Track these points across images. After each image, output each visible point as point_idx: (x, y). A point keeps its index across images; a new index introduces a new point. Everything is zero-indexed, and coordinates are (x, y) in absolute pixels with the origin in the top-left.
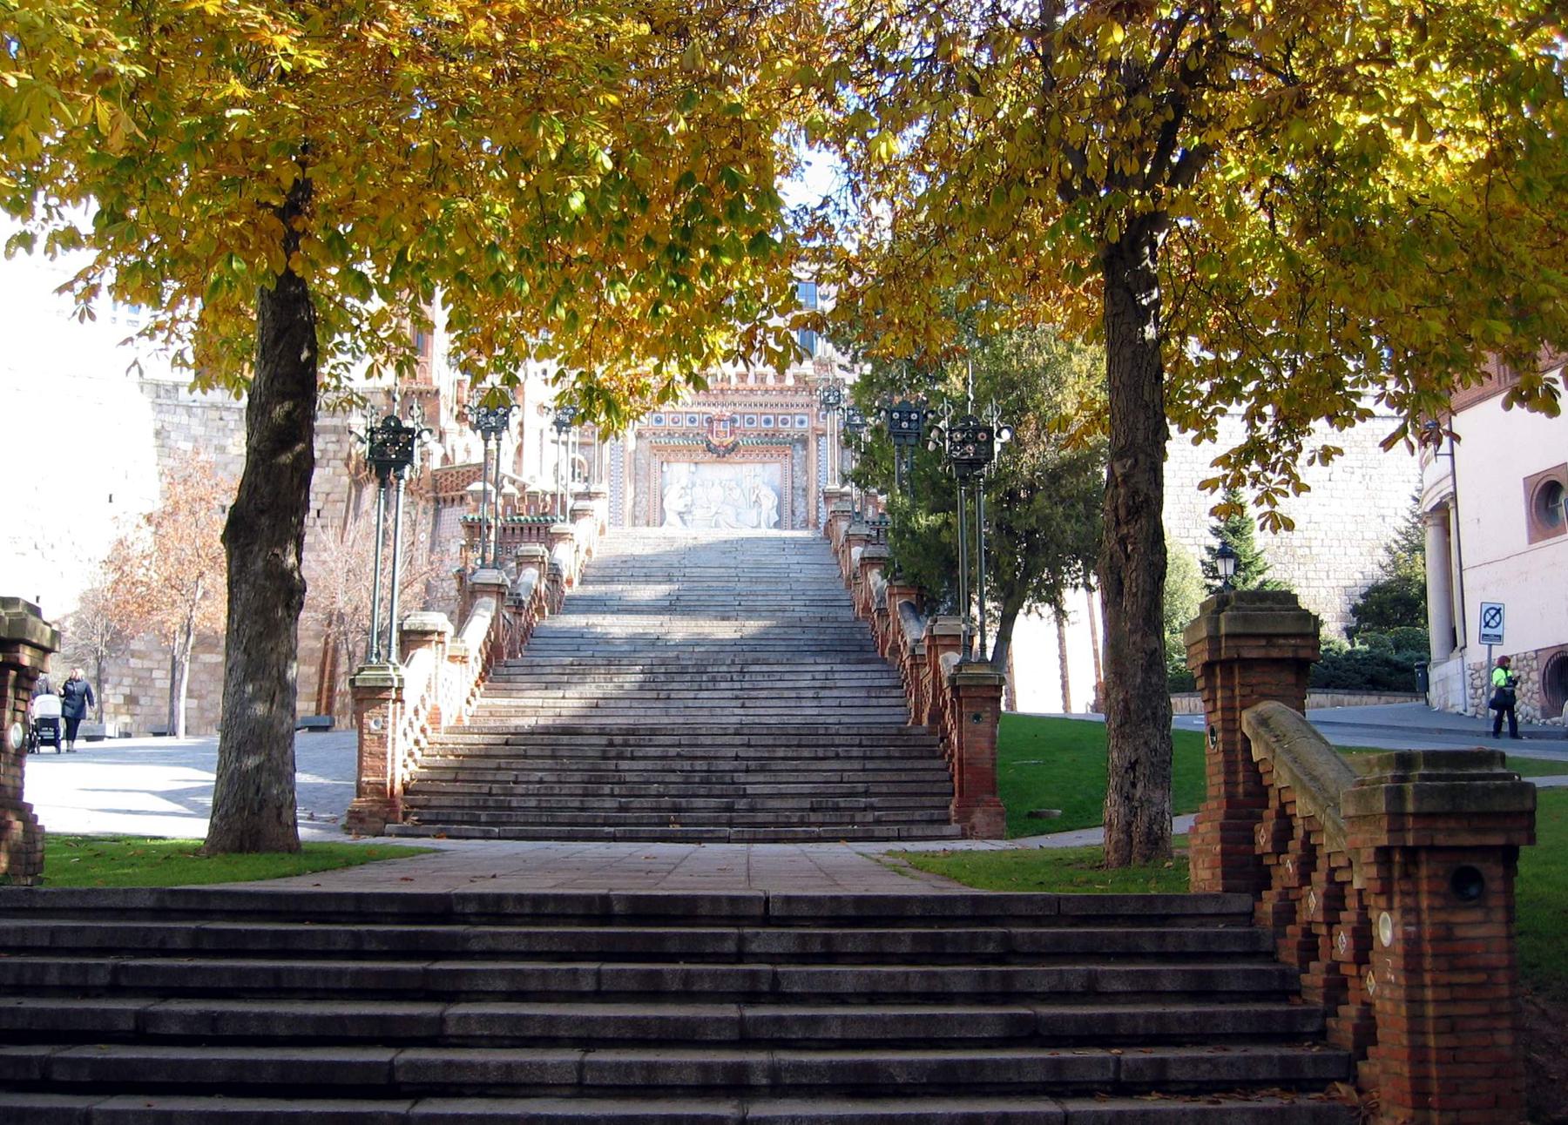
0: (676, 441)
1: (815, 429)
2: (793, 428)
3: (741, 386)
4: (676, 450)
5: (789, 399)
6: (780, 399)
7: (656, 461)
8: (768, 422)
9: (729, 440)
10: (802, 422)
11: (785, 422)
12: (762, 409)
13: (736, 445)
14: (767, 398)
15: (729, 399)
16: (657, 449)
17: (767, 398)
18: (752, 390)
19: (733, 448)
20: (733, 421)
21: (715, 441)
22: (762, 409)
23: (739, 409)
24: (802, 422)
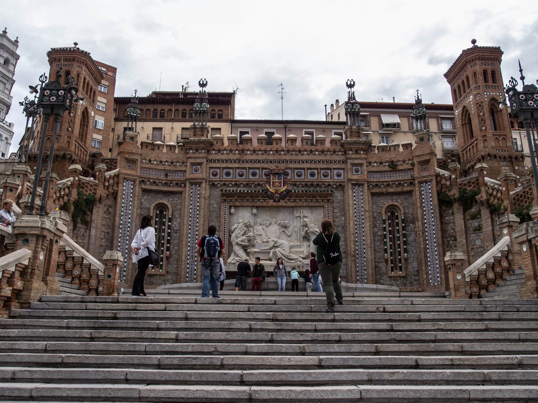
0: (242, 189)
1: (349, 180)
2: (333, 178)
3: (291, 147)
4: (241, 196)
5: (328, 157)
6: (322, 157)
7: (225, 207)
8: (312, 175)
9: (283, 189)
10: (339, 175)
11: (326, 176)
12: (308, 165)
13: (288, 192)
14: (311, 157)
15: (284, 157)
16: (226, 196)
17: (311, 157)
18: (300, 151)
19: (286, 195)
20: (287, 174)
21: (272, 190)
22: (308, 165)
23: (291, 166)
24: (339, 175)
